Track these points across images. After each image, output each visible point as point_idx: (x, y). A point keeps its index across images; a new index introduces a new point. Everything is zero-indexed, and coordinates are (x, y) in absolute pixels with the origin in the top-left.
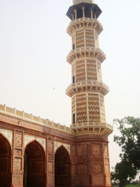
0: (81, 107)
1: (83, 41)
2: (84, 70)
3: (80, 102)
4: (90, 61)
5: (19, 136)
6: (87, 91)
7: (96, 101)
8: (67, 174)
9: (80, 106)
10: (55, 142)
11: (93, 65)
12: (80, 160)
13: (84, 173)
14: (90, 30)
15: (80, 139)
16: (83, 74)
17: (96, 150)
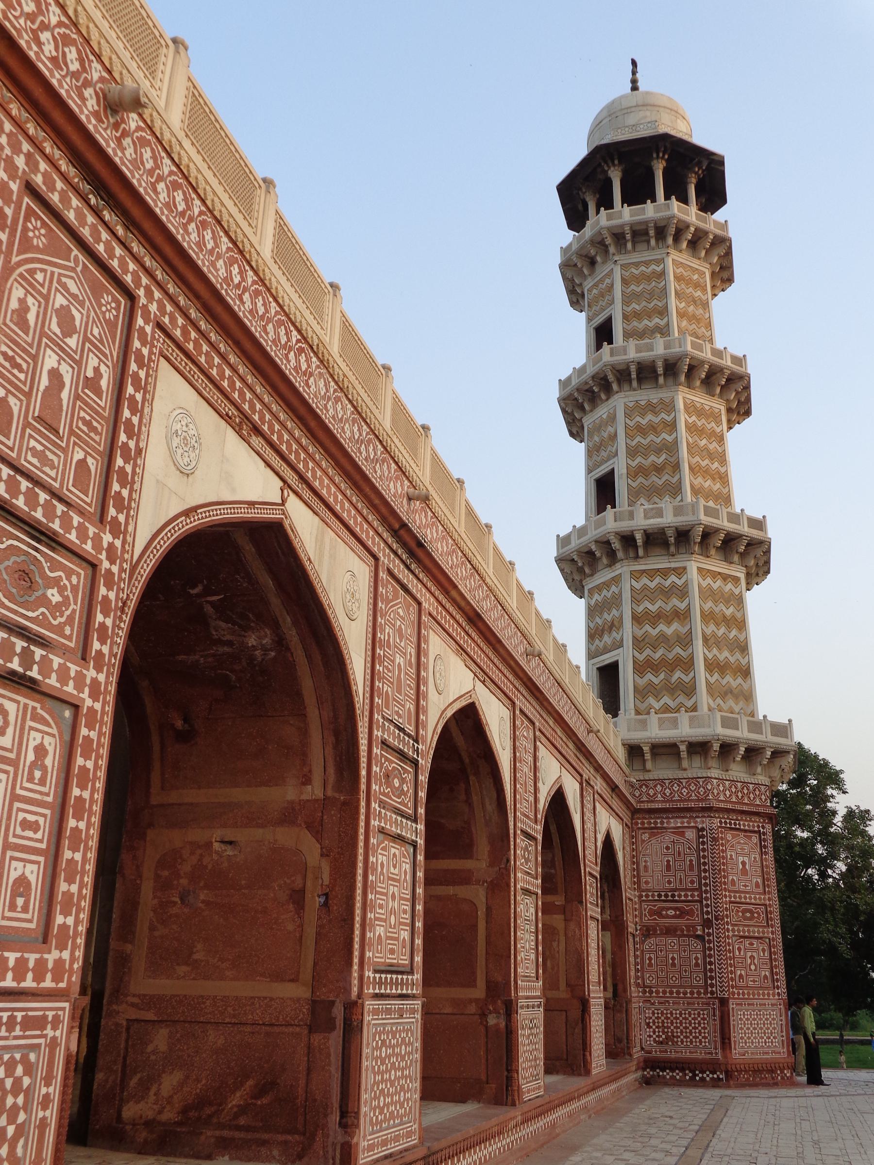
3: (653, 608)
4: (700, 413)
9: (654, 625)
11: (713, 433)
13: (681, 986)
15: (659, 797)
16: (669, 469)
17: (744, 863)
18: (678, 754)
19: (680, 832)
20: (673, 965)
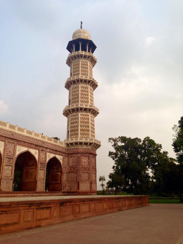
0: (74, 126)
1: (79, 71)
2: (78, 94)
4: (84, 88)
5: (10, 147)
6: (79, 112)
7: (87, 120)
8: (59, 181)
9: (73, 124)
10: (48, 154)
12: (71, 169)
14: (85, 62)
18: (73, 145)
19: (75, 157)
20: (72, 177)
